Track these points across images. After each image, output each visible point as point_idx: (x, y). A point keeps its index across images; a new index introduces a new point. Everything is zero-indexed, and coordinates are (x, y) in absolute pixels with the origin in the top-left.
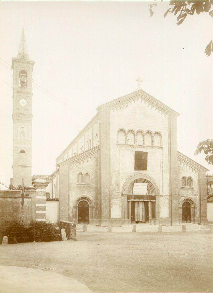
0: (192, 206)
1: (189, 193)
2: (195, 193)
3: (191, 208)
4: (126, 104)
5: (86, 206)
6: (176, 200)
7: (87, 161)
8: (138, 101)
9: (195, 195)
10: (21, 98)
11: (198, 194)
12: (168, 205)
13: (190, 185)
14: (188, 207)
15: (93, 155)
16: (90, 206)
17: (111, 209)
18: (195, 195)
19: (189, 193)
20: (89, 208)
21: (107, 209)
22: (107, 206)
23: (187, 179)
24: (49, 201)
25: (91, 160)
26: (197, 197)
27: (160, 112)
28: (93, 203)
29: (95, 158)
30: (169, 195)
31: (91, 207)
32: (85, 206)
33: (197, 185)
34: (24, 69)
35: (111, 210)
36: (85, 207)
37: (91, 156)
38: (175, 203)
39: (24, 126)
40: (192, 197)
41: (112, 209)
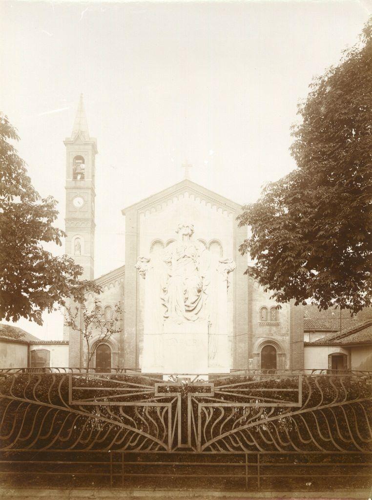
0: (278, 352)
1: (272, 332)
2: (284, 331)
3: (277, 356)
4: (159, 206)
5: (108, 352)
6: (245, 343)
7: (109, 289)
8: (184, 197)
9: (283, 335)
10: (76, 197)
11: (289, 333)
12: (231, 350)
13: (276, 319)
14: (273, 353)
15: (117, 279)
16: (112, 351)
17: (139, 356)
18: (283, 335)
19: (272, 332)
20: (112, 355)
21: (133, 356)
22: (132, 351)
23: (269, 310)
24: (57, 345)
25: (114, 287)
26: (288, 338)
27: (220, 210)
28: (116, 347)
29: (120, 284)
30: (232, 335)
31: (113, 353)
32: (107, 351)
33: (288, 318)
34: (79, 154)
35: (140, 357)
36: (107, 353)
37: (113, 282)
38: (241, 348)
39: (78, 236)
40: (277, 338)
41: (140, 356)
